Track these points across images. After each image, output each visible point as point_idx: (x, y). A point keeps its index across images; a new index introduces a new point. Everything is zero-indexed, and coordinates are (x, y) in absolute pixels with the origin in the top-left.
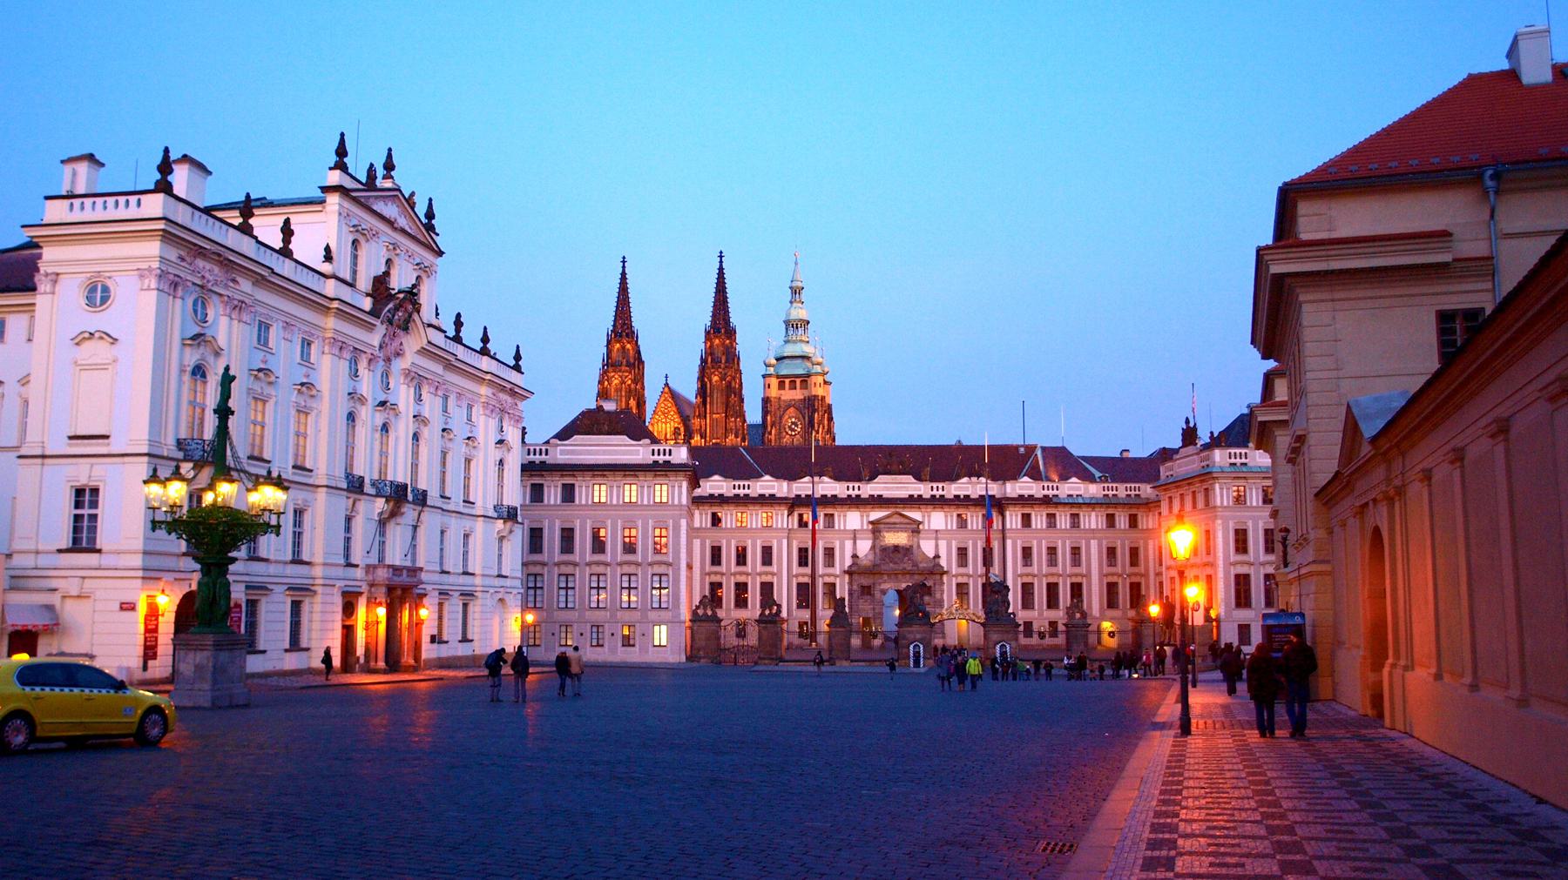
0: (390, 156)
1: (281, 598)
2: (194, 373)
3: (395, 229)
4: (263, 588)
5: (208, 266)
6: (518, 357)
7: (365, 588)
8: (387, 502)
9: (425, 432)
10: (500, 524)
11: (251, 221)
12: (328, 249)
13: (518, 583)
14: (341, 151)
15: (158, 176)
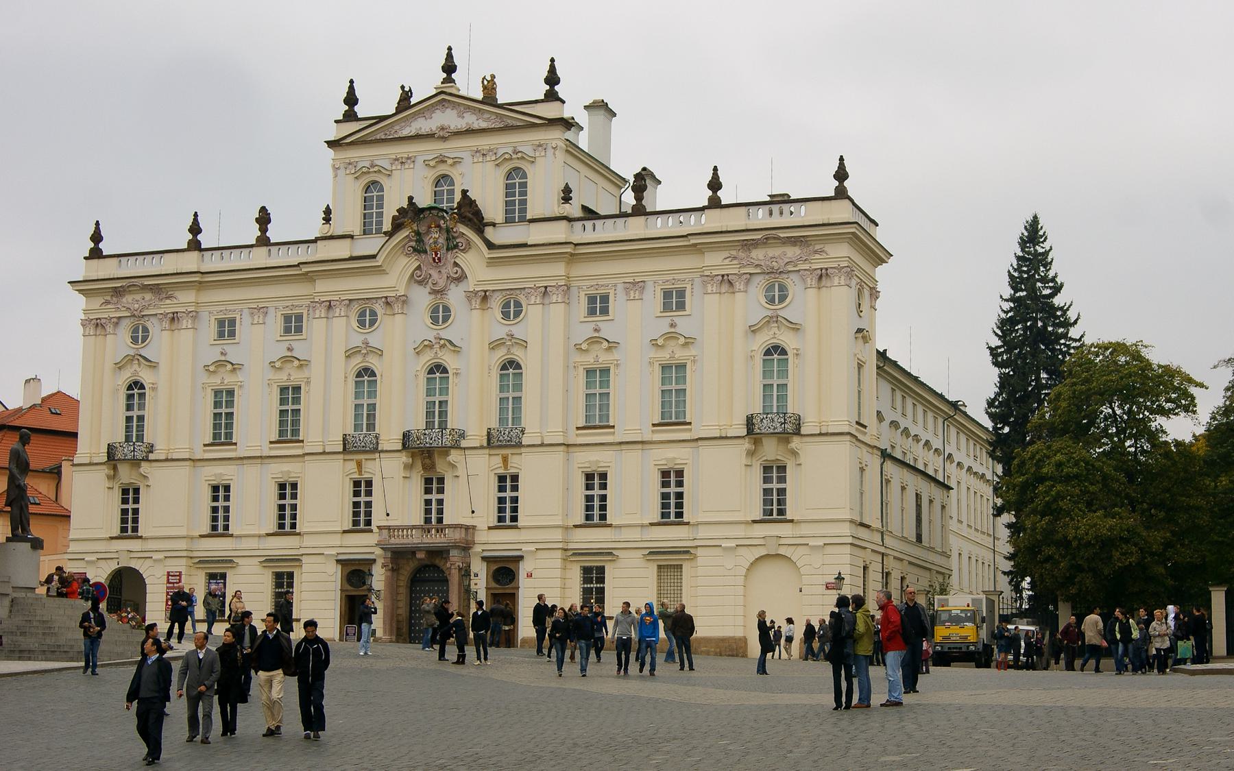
0: (450, 56)
1: (258, 569)
2: (130, 388)
3: (444, 139)
4: (229, 561)
5: (138, 297)
6: (841, 175)
7: (378, 551)
8: (412, 457)
9: (530, 361)
10: (746, 445)
11: (199, 237)
12: (328, 212)
13: (846, 529)
14: (351, 99)
15: (92, 245)
